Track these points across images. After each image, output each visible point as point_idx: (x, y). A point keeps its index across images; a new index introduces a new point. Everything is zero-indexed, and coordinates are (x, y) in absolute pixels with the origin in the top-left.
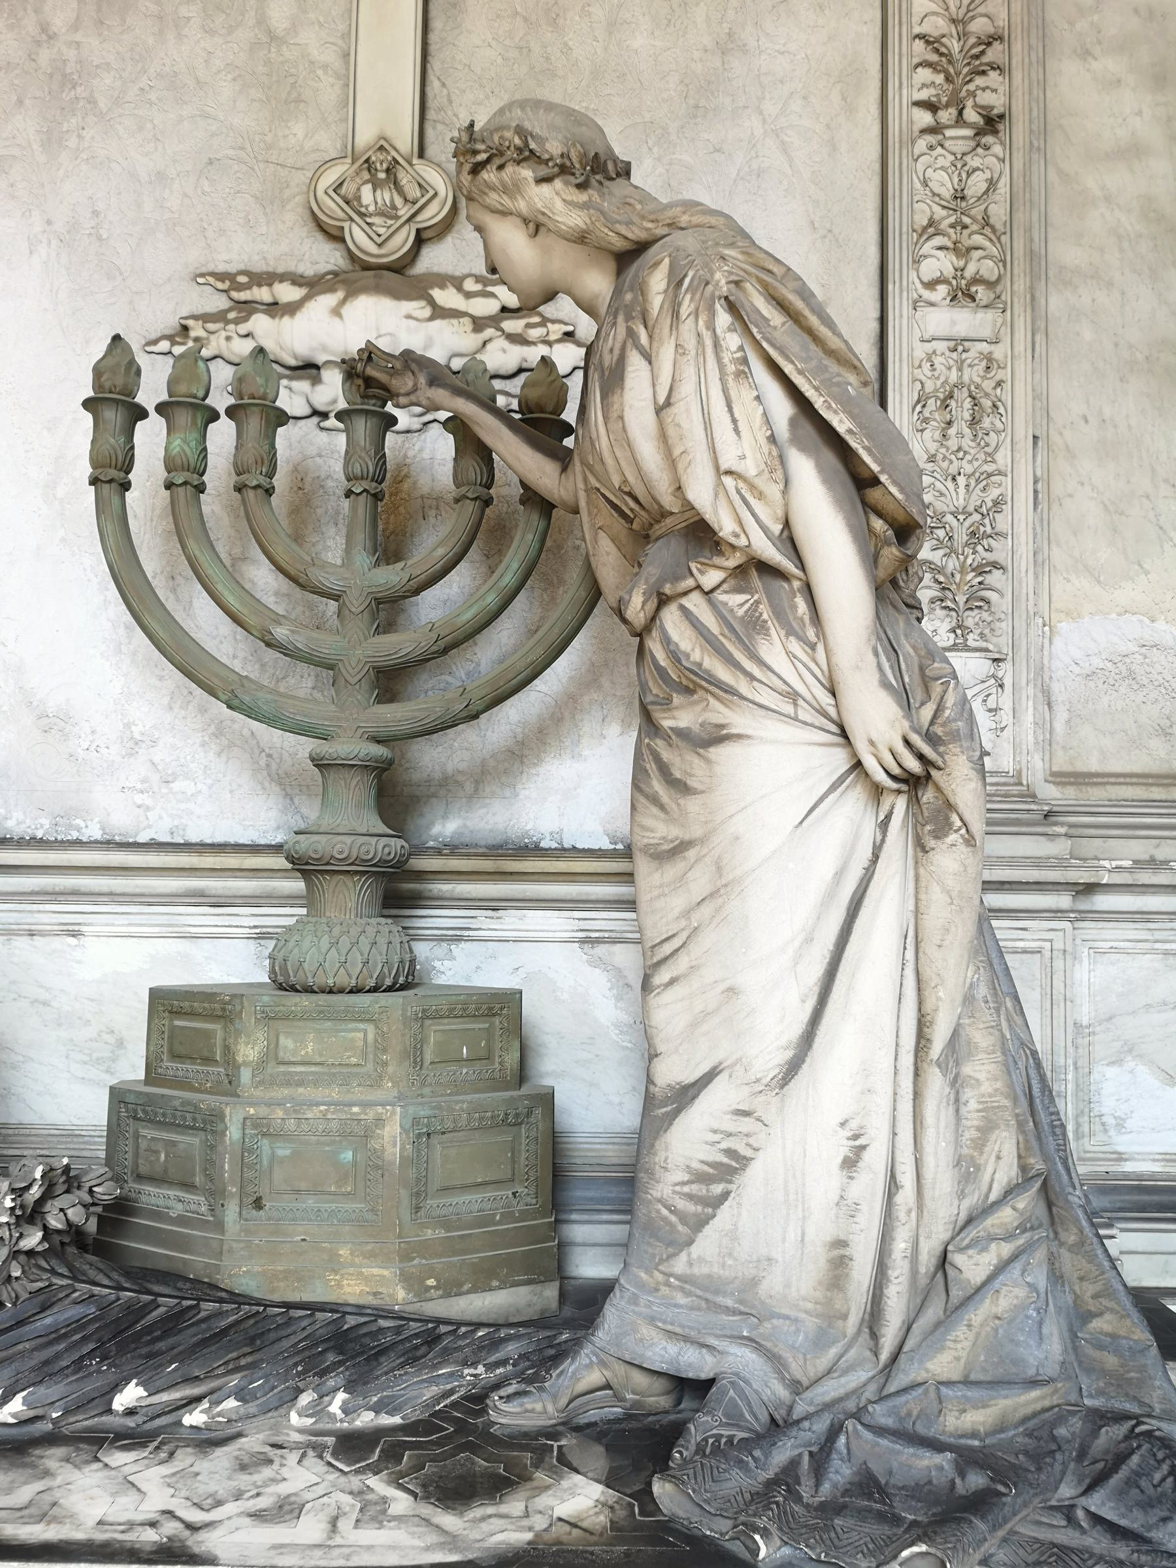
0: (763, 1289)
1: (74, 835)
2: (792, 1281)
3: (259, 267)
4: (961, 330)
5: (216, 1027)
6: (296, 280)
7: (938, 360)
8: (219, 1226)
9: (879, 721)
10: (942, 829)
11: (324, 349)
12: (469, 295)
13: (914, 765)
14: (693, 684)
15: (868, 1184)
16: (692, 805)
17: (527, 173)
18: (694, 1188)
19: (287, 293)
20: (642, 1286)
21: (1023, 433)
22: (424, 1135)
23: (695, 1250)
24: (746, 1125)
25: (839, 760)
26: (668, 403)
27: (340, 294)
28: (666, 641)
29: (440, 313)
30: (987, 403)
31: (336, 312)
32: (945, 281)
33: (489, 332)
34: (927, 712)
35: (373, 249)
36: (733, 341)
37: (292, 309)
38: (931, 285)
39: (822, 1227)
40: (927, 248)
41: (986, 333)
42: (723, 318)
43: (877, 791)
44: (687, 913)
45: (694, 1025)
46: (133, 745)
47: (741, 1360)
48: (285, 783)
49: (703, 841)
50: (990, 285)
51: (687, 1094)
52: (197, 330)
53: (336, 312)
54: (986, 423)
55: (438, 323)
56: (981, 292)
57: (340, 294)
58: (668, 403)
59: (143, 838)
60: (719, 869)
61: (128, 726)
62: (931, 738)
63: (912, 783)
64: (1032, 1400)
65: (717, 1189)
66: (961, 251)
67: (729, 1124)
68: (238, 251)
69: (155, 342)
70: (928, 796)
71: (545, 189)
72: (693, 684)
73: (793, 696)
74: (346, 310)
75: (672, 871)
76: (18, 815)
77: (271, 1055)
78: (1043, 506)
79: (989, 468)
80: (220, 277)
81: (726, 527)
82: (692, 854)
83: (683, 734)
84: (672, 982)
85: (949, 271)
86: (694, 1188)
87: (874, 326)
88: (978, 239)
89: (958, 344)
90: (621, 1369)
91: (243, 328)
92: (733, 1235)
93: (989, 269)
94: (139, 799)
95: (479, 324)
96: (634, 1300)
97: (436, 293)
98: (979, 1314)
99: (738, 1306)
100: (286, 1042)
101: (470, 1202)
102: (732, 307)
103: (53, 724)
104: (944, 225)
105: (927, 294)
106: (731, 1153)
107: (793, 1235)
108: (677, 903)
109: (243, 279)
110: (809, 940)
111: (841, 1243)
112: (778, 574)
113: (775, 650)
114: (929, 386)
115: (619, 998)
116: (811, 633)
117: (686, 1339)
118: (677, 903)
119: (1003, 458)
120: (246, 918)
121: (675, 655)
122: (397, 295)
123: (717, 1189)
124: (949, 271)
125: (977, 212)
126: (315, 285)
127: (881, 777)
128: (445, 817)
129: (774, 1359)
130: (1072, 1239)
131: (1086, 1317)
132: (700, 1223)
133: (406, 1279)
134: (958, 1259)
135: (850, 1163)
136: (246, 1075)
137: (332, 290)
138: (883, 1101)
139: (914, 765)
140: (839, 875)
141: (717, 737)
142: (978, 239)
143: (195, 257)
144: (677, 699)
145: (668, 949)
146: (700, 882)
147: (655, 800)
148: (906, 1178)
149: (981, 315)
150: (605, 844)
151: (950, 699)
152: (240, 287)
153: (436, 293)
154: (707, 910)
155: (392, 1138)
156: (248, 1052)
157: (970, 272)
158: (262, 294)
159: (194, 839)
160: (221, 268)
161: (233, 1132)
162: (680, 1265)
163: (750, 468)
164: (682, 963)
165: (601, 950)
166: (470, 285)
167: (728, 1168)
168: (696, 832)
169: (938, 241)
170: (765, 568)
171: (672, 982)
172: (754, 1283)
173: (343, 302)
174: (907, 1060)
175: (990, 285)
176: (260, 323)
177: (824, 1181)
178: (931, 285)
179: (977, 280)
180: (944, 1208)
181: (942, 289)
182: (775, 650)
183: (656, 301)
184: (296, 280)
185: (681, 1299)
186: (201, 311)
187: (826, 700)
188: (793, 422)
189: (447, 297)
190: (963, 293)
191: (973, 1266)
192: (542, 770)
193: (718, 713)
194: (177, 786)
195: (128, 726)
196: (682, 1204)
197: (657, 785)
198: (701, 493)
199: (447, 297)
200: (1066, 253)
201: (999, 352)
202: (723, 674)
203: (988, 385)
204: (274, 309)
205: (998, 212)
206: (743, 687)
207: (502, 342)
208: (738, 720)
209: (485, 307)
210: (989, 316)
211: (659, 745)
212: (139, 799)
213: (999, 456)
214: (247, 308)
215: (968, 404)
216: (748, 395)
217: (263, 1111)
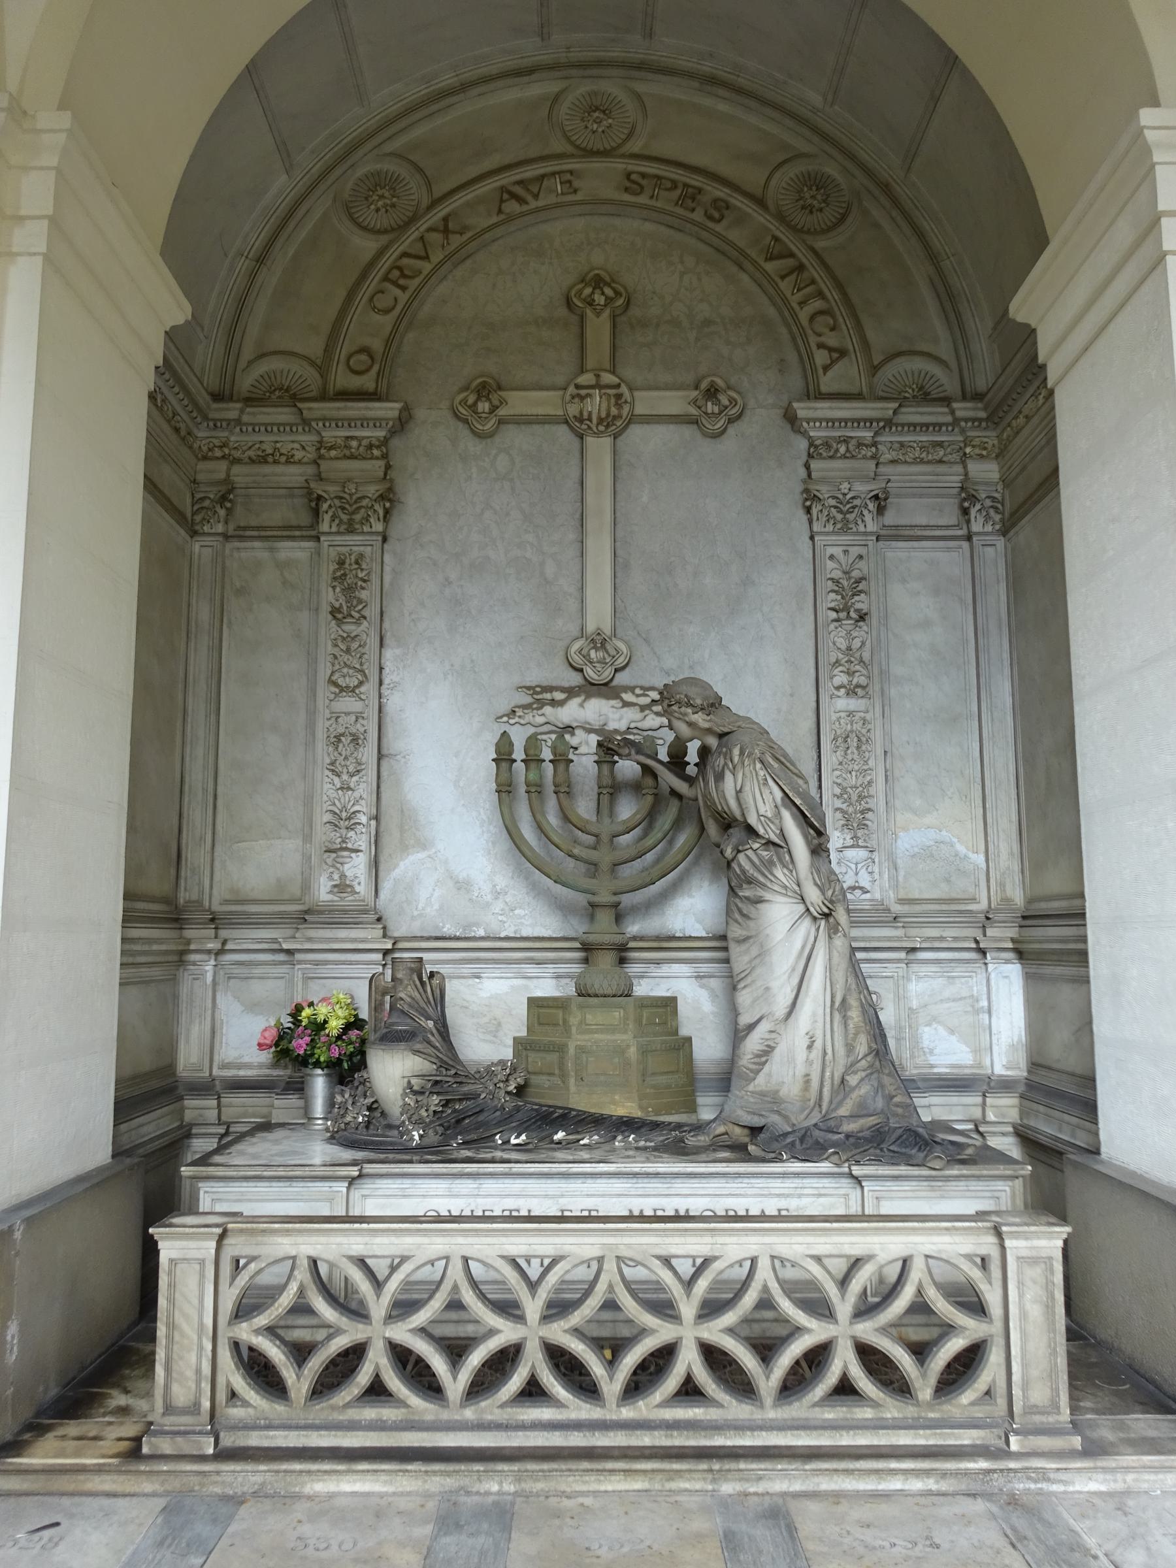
0: (781, 1094)
1: (473, 934)
2: (791, 1089)
3: (545, 684)
4: (852, 708)
5: (560, 1013)
6: (562, 690)
7: (842, 721)
8: (568, 1089)
9: (813, 895)
10: (836, 932)
11: (576, 720)
12: (638, 696)
13: (826, 910)
14: (750, 881)
15: (816, 1053)
16: (751, 924)
17: (689, 710)
18: (756, 1060)
19: (559, 696)
20: (737, 1096)
21: (880, 752)
22: (644, 1052)
23: (756, 1082)
24: (773, 1035)
25: (802, 908)
26: (740, 791)
27: (583, 698)
28: (740, 865)
29: (626, 704)
30: (864, 739)
31: (581, 705)
32: (844, 687)
33: (647, 712)
34: (830, 893)
35: (596, 677)
36: (762, 773)
37: (562, 703)
38: (838, 688)
39: (801, 1070)
40: (836, 672)
41: (863, 708)
42: (758, 765)
43: (815, 919)
44: (750, 962)
45: (754, 1001)
46: (497, 894)
47: (775, 1118)
48: (564, 909)
49: (756, 936)
50: (864, 688)
51: (751, 1027)
52: (519, 712)
53: (581, 705)
54: (864, 747)
55: (625, 709)
56: (859, 691)
57: (583, 698)
58: (740, 791)
59: (502, 935)
60: (762, 946)
61: (494, 886)
62: (831, 902)
63: (826, 916)
64: (872, 1121)
65: (764, 1059)
66: (850, 673)
67: (767, 1036)
68: (535, 677)
69: (501, 717)
70: (831, 920)
71: (696, 716)
72: (750, 881)
73: (786, 887)
74: (586, 705)
75: (744, 947)
76: (448, 926)
77: (583, 1022)
78: (890, 781)
79: (865, 767)
80: (528, 688)
81: (761, 831)
82: (751, 941)
83: (747, 898)
84: (745, 987)
85: (846, 682)
86: (756, 1060)
87: (814, 704)
88: (858, 667)
89: (850, 714)
90: (731, 1126)
91: (540, 712)
92: (770, 1075)
93: (863, 681)
94: (500, 918)
95: (643, 708)
96: (735, 1102)
97: (624, 696)
98: (854, 1095)
99: (772, 1099)
100: (589, 1017)
101: (662, 1080)
102: (762, 762)
103: (463, 886)
104: (843, 662)
105: (836, 692)
106: (768, 1046)
107: (791, 1073)
108: (746, 958)
109: (538, 689)
110: (793, 970)
111: (808, 1075)
112: (779, 846)
113: (779, 872)
114: (839, 732)
115: (713, 1001)
116: (791, 867)
117: (754, 1114)
118: (746, 958)
119: (871, 763)
120: (551, 969)
121: (743, 871)
122: (608, 698)
123: (764, 1059)
124: (846, 682)
125: (857, 655)
126: (571, 692)
127: (816, 914)
128: (633, 923)
129: (786, 1118)
130: (887, 1071)
131: (892, 1097)
132: (758, 1072)
133: (641, 1108)
134: (848, 1078)
135: (810, 1047)
136: (574, 1029)
137: (578, 695)
138: (820, 1025)
139: (826, 910)
140: (803, 947)
141: (759, 901)
142: (858, 667)
143: (517, 680)
144: (745, 886)
145: (743, 975)
146: (754, 951)
147: (736, 921)
148: (829, 1051)
149: (860, 701)
150: (704, 934)
151: (837, 888)
152: (538, 693)
153: (624, 696)
154: (757, 961)
155: (633, 1052)
156: (574, 1020)
157: (854, 682)
158: (548, 696)
159: (524, 934)
160: (528, 684)
161: (572, 1051)
162: (751, 1088)
163: (769, 815)
164: (749, 980)
165: (705, 980)
166: (638, 691)
167: (768, 1051)
168: (753, 933)
169: (841, 668)
170: (774, 844)
171: (745, 987)
172: (777, 1092)
173: (584, 701)
174: (828, 1010)
175: (864, 688)
176: (548, 710)
177: (801, 1054)
178: (838, 688)
179: (858, 686)
180: (842, 1062)
181: (843, 691)
182: (779, 872)
183: (736, 759)
184: (562, 690)
185: (752, 1100)
186: (520, 703)
187: (797, 888)
188: (782, 799)
189: (628, 697)
190: (851, 692)
191: (853, 1080)
192: (675, 902)
193: (761, 892)
194: (516, 912)
195: (494, 886)
196: (751, 1066)
197: (737, 916)
198: (752, 820)
199: (628, 697)
200: (897, 670)
201: (868, 716)
202: (761, 879)
203: (864, 731)
204: (554, 703)
205: (866, 656)
206: (769, 884)
207: (653, 716)
208: (767, 896)
209: (647, 700)
210: (864, 701)
211: (737, 901)
212: (500, 918)
213: (870, 762)
214: (541, 704)
215: (856, 739)
216: (768, 792)
217: (583, 1043)
